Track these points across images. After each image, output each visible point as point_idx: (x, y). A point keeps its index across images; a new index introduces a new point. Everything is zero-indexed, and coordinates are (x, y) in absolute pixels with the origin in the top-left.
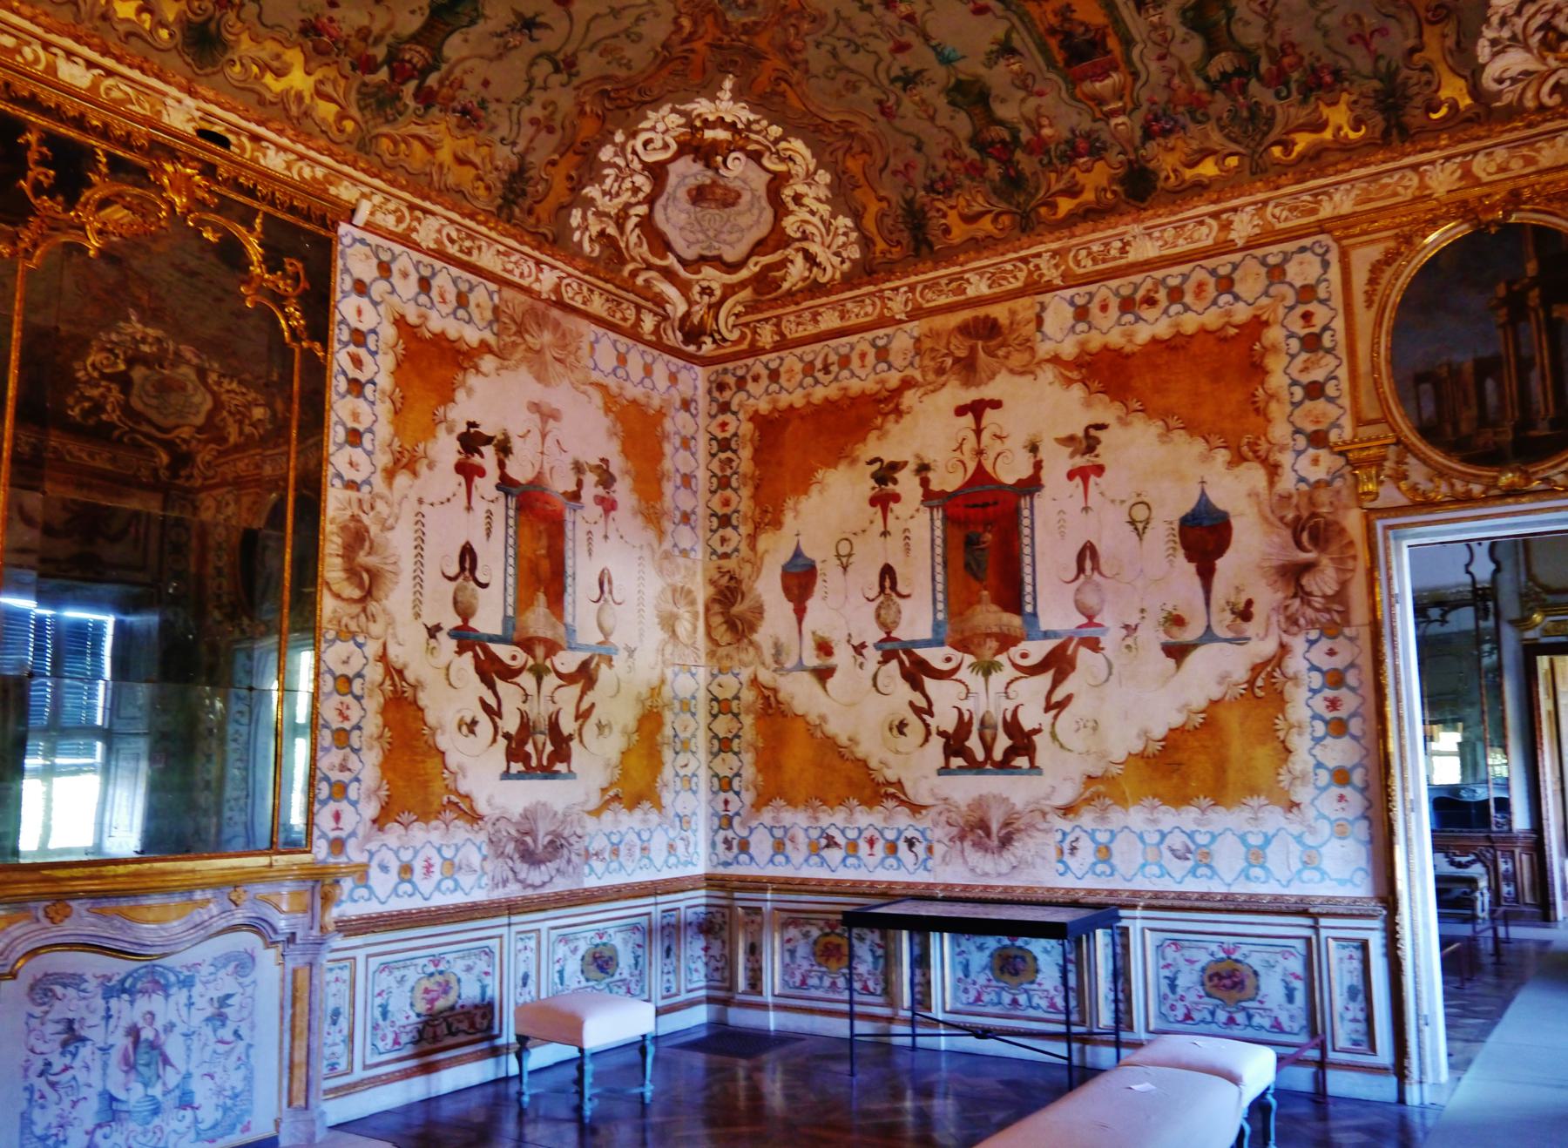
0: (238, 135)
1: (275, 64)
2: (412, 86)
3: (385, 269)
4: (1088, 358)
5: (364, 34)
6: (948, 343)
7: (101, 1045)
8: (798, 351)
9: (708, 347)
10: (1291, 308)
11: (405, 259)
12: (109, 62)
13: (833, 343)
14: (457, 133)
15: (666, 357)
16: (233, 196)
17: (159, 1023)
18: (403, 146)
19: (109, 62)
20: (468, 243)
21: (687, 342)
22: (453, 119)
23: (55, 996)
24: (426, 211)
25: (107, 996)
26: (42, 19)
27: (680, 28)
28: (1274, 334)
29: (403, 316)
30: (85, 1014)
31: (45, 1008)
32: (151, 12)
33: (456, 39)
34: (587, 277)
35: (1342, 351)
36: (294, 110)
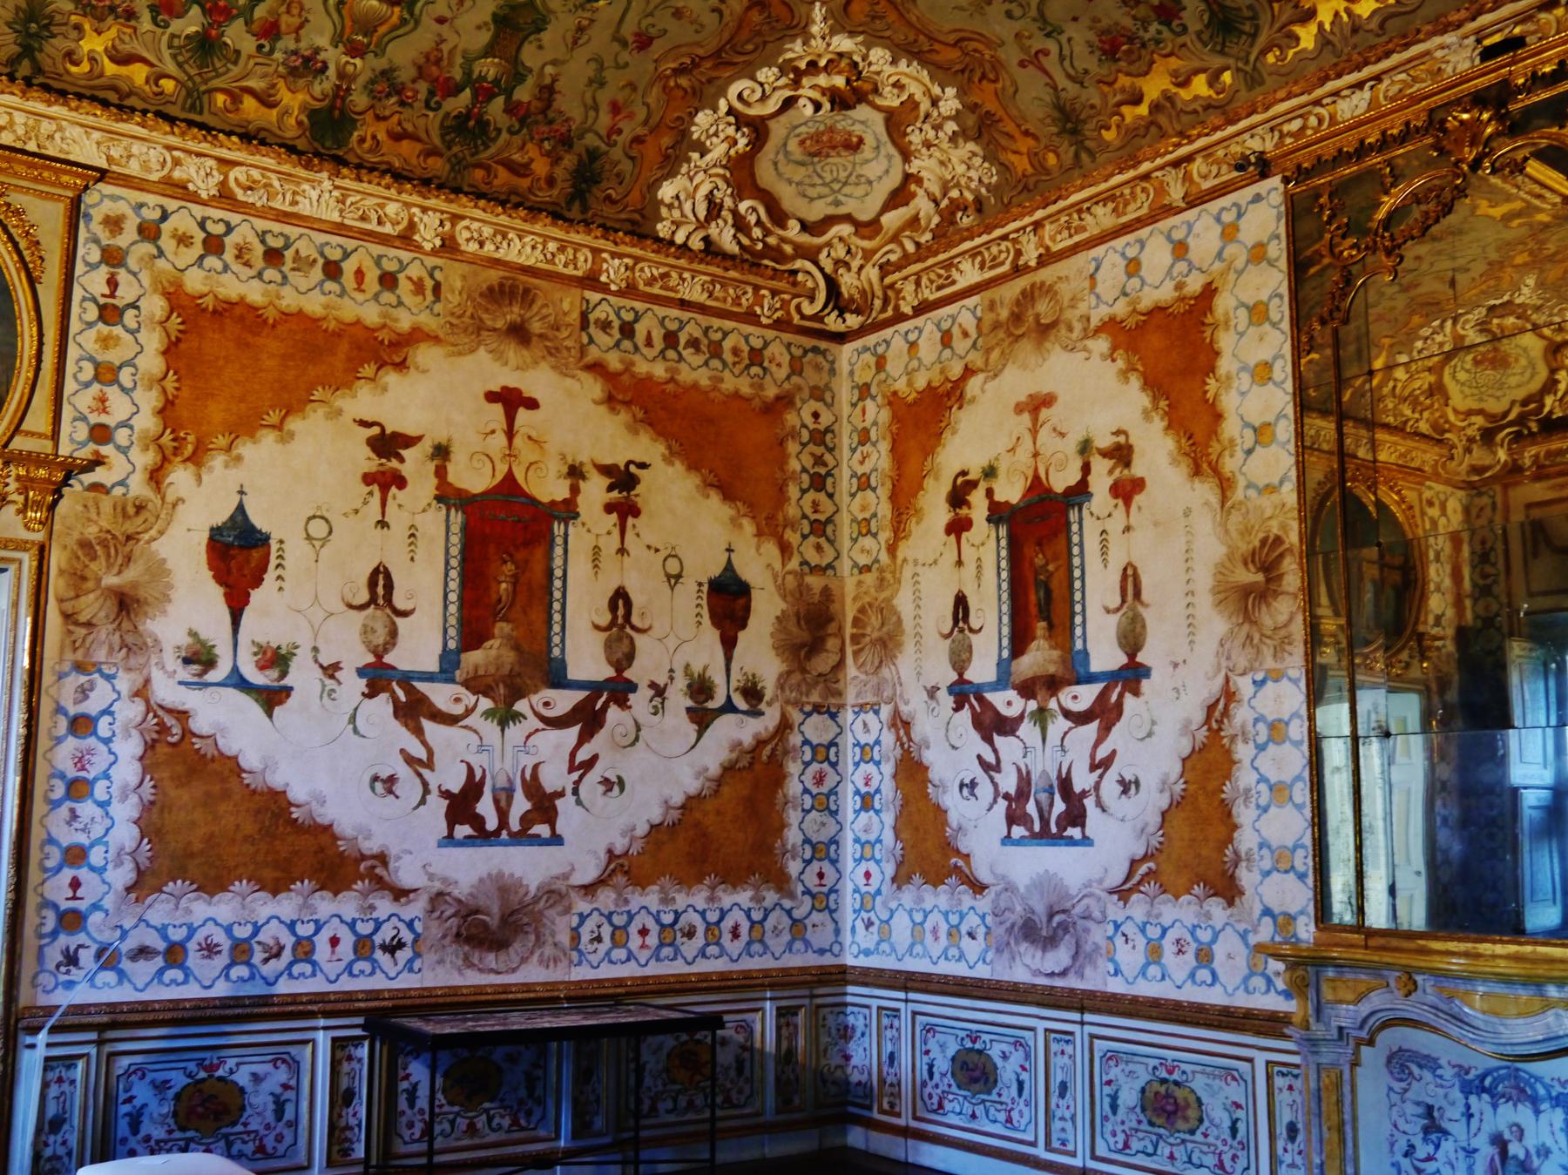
0: (1529, 18)
7: (1464, 1144)
17: (1531, 1141)
19: (1367, 71)
23: (1411, 1073)
25: (1468, 1089)
26: (1296, 89)
30: (1443, 1103)
31: (1403, 1085)
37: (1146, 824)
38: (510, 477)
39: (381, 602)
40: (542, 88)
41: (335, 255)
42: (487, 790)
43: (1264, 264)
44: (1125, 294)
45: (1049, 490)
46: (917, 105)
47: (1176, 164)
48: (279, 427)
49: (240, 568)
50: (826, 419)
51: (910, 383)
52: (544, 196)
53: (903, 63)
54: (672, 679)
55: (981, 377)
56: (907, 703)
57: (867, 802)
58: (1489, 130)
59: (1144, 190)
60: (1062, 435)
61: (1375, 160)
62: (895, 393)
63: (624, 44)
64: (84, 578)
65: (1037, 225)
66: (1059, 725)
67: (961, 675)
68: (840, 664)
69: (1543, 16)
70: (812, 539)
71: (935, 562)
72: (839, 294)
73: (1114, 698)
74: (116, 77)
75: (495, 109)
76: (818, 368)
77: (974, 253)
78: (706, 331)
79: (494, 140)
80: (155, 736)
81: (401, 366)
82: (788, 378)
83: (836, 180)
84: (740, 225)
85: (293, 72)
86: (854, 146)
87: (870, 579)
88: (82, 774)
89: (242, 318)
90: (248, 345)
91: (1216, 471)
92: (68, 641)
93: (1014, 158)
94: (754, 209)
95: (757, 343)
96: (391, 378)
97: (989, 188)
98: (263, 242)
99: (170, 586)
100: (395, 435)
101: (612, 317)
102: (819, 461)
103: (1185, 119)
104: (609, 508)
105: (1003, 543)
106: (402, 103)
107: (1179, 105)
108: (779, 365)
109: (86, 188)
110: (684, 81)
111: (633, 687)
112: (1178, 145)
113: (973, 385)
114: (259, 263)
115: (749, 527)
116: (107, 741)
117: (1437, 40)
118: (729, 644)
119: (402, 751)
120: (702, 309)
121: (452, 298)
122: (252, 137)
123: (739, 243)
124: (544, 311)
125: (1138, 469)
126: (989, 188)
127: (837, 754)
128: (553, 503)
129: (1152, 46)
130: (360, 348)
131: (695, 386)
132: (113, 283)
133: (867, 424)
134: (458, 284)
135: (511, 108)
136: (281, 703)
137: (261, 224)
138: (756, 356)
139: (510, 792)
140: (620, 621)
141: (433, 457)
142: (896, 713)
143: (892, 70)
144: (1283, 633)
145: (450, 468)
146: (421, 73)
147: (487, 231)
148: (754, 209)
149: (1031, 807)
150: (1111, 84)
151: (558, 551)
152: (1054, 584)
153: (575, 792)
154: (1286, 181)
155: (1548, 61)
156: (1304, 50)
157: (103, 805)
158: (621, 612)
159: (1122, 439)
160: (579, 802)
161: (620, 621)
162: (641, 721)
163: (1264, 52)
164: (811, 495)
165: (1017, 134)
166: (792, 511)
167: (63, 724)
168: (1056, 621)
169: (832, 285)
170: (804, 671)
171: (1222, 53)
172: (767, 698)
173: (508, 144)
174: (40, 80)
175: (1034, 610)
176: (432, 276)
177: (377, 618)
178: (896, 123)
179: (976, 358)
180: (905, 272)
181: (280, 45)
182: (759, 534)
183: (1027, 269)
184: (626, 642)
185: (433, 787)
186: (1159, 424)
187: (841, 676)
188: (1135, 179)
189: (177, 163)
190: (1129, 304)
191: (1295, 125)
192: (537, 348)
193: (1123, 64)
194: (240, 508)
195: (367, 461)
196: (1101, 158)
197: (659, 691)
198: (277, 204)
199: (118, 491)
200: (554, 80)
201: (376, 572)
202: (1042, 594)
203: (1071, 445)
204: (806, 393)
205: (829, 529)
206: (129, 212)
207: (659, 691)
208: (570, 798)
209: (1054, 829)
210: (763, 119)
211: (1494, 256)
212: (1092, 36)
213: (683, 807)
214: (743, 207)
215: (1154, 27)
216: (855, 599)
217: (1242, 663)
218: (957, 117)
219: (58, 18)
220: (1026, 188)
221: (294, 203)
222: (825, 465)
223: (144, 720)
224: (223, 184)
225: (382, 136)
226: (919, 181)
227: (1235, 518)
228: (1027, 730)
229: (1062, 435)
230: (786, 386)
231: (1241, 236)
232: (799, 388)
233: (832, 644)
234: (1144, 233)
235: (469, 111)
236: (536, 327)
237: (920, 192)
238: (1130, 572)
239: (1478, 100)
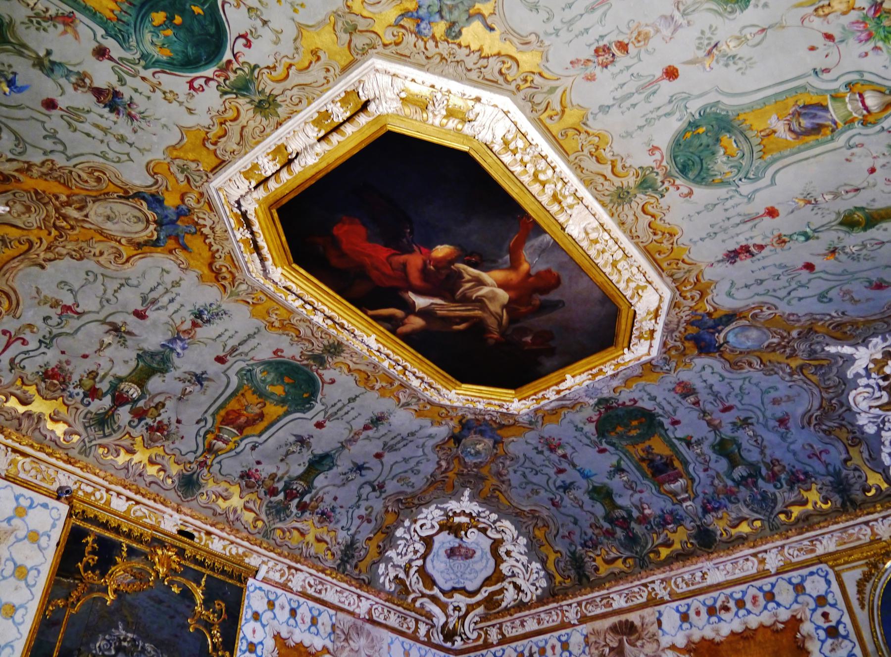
0: (200, 532)
1: (225, 494)
2: (296, 501)
3: (271, 604)
4: (693, 646)
5: (273, 477)
6: (605, 638)
8: (514, 645)
9: (459, 644)
10: (814, 610)
11: (283, 598)
12: (138, 498)
13: (535, 639)
14: (318, 525)
15: (434, 651)
16: (192, 566)
18: (288, 534)
19: (138, 498)
20: (320, 587)
21: (445, 640)
22: (316, 518)
24: (297, 570)
26: (109, 478)
27: (441, 466)
28: (807, 628)
29: (279, 633)
32: (165, 471)
33: (321, 477)
34: (387, 604)
35: (853, 636)
36: (231, 517)
43: (36, 546)
47: (15, 451)
107: (41, 425)
129: (66, 394)
150: (23, 383)
156: (116, 462)
163: (101, 446)
171: (86, 428)
191: (89, 489)
193: (43, 385)
212: (53, 364)
231: (27, 519)
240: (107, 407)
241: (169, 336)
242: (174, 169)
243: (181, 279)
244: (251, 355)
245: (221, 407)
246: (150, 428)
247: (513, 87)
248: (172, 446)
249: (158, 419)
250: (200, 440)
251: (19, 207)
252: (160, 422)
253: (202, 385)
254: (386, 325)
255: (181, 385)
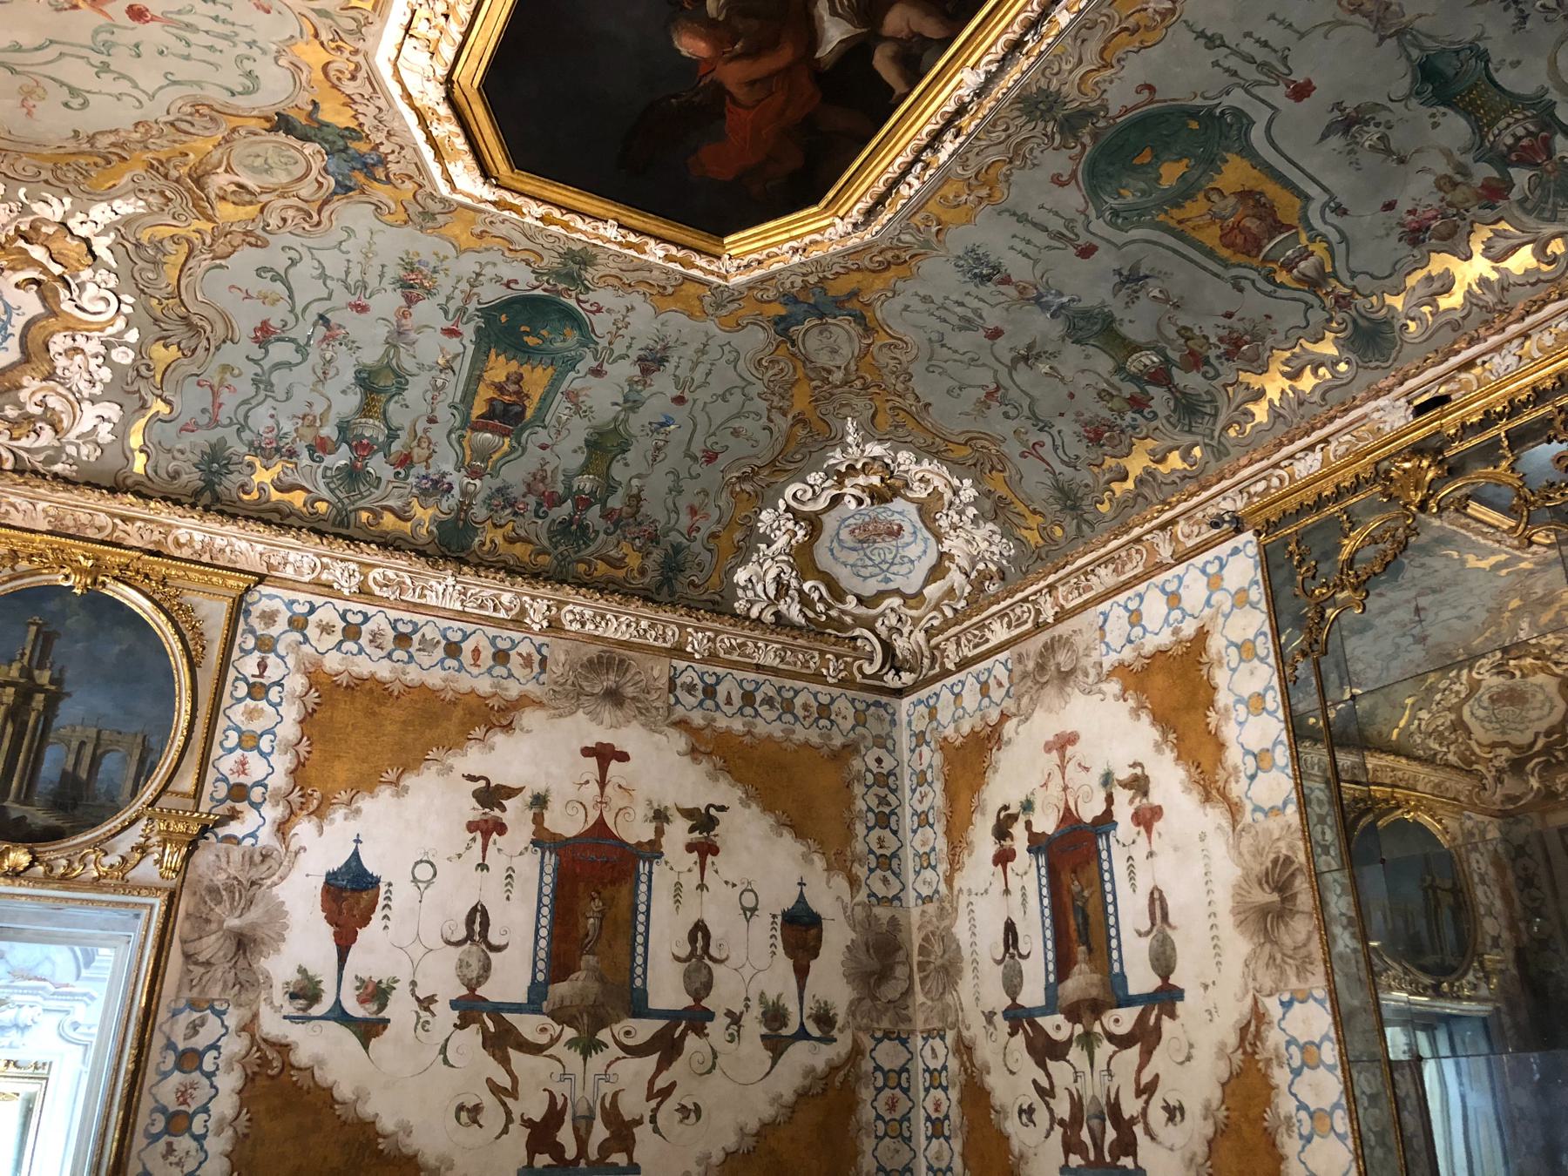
1: (1436, 285)
5: (1445, 184)
12: (1315, 436)
19: (1315, 436)
26: (1256, 456)
32: (1322, 365)
33: (1506, 78)
36: (1490, 298)
37: (1194, 1155)
38: (601, 822)
39: (477, 938)
40: (630, 497)
41: (455, 637)
42: (568, 1118)
44: (1130, 642)
45: (1079, 821)
46: (941, 495)
47: (1163, 527)
48: (395, 783)
49: (351, 909)
50: (888, 763)
51: (957, 730)
52: (638, 582)
53: (926, 462)
54: (747, 1007)
55: (1015, 721)
56: (968, 1028)
57: (937, 1127)
58: (1430, 475)
59: (1138, 551)
60: (1087, 769)
61: (1333, 509)
62: (945, 739)
63: (695, 459)
64: (208, 921)
65: (1051, 588)
66: (1105, 1049)
67: (1014, 1000)
68: (909, 992)
69: (1463, 376)
70: (878, 872)
71: (986, 891)
72: (894, 655)
73: (1152, 1020)
74: (279, 501)
75: (593, 515)
76: (880, 719)
77: (1002, 615)
78: (779, 690)
79: (594, 540)
80: (256, 1069)
81: (508, 728)
82: (853, 728)
83: (884, 561)
84: (805, 601)
85: (424, 493)
86: (897, 533)
87: (931, 908)
88: (183, 1108)
89: (371, 691)
90: (374, 714)
91: (1225, 797)
92: (186, 980)
93: (1025, 533)
94: (817, 588)
95: (825, 700)
96: (499, 738)
97: (1008, 559)
98: (394, 628)
99: (286, 927)
100: (498, 787)
101: (697, 681)
102: (883, 801)
103: (1165, 489)
104: (690, 848)
105: (1043, 871)
106: (515, 514)
107: (1160, 478)
108: (845, 718)
109: (248, 589)
110: (747, 487)
111: (710, 1016)
112: (1162, 511)
113: (1009, 728)
114: (389, 644)
115: (819, 863)
116: (209, 1076)
117: (1373, 404)
118: (802, 972)
119: (489, 1080)
120: (775, 671)
121: (556, 670)
122: (390, 544)
123: (805, 616)
124: (637, 678)
125: (1155, 798)
126: (1008, 559)
127: (908, 1080)
128: (639, 844)
129: (1130, 431)
130: (472, 714)
131: (770, 737)
132: (263, 666)
133: (924, 767)
134: (562, 658)
135: (607, 514)
136: (377, 1035)
137: (393, 614)
138: (824, 711)
139: (590, 1119)
140: (699, 952)
141: (532, 805)
142: (959, 1038)
143: (918, 468)
144: (1303, 952)
145: (547, 815)
146: (530, 489)
147: (588, 613)
148: (817, 588)
149: (1085, 1135)
151: (643, 888)
152: (1090, 910)
153: (653, 1120)
154: (1258, 533)
155: (1475, 411)
156: (1260, 423)
157: (199, 1139)
158: (700, 944)
159: (1138, 771)
160: (656, 1130)
161: (699, 952)
162: (717, 1048)
163: (1226, 428)
164: (877, 832)
165: (1027, 513)
166: (860, 847)
167: (171, 1058)
168: (1095, 946)
169: (888, 648)
170: (874, 998)
171: (1190, 432)
172: (838, 1025)
173: (605, 543)
174: (219, 506)
175: (1074, 935)
176: (539, 652)
177: (472, 951)
178: (927, 511)
179: (1010, 705)
180: (947, 634)
181: (413, 472)
182: (829, 868)
183: (1046, 625)
184: (705, 972)
185: (516, 1116)
186: (1169, 755)
187: (910, 1002)
188: (1129, 542)
189: (325, 567)
190: (1134, 650)
191: (1261, 486)
192: (630, 709)
194: (356, 854)
195: (472, 810)
196: (1098, 527)
197: (735, 1019)
198: (408, 597)
199: (249, 842)
200: (640, 490)
201: (474, 909)
202: (1080, 920)
203: (1094, 778)
204: (869, 742)
205: (895, 863)
206: (283, 608)
207: (735, 1019)
208: (648, 1126)
209: (1108, 1159)
210: (817, 514)
211: (1492, 604)
212: (1078, 428)
213: (758, 1134)
214: (806, 586)
215: (1129, 416)
216: (919, 928)
217: (1268, 984)
218: (975, 503)
219: (235, 459)
220: (1039, 557)
221: (422, 596)
222: (889, 804)
223: (248, 1053)
224: (363, 583)
225: (499, 540)
226: (951, 558)
227: (1247, 841)
228: (1076, 1054)
229: (1087, 769)
230: (852, 735)
231: (1225, 585)
232: (864, 737)
233: (900, 971)
234: (1141, 588)
235: (572, 518)
236: (629, 691)
237: (953, 567)
238: (1156, 895)
239: (1417, 450)
240: (1168, 395)
241: (1037, 309)
242: (724, 312)
243: (916, 294)
244: (1070, 214)
245: (1210, 253)
246: (1228, 356)
247: (359, 58)
248: (1280, 336)
249: (1213, 340)
250: (1280, 292)
251: (845, 411)
252: (1221, 340)
253: (1147, 277)
254: (926, 57)
255: (1143, 302)
